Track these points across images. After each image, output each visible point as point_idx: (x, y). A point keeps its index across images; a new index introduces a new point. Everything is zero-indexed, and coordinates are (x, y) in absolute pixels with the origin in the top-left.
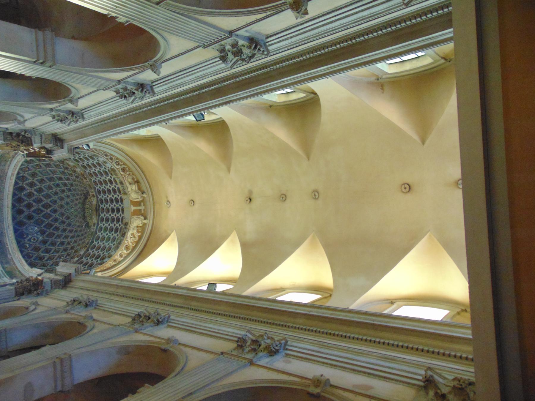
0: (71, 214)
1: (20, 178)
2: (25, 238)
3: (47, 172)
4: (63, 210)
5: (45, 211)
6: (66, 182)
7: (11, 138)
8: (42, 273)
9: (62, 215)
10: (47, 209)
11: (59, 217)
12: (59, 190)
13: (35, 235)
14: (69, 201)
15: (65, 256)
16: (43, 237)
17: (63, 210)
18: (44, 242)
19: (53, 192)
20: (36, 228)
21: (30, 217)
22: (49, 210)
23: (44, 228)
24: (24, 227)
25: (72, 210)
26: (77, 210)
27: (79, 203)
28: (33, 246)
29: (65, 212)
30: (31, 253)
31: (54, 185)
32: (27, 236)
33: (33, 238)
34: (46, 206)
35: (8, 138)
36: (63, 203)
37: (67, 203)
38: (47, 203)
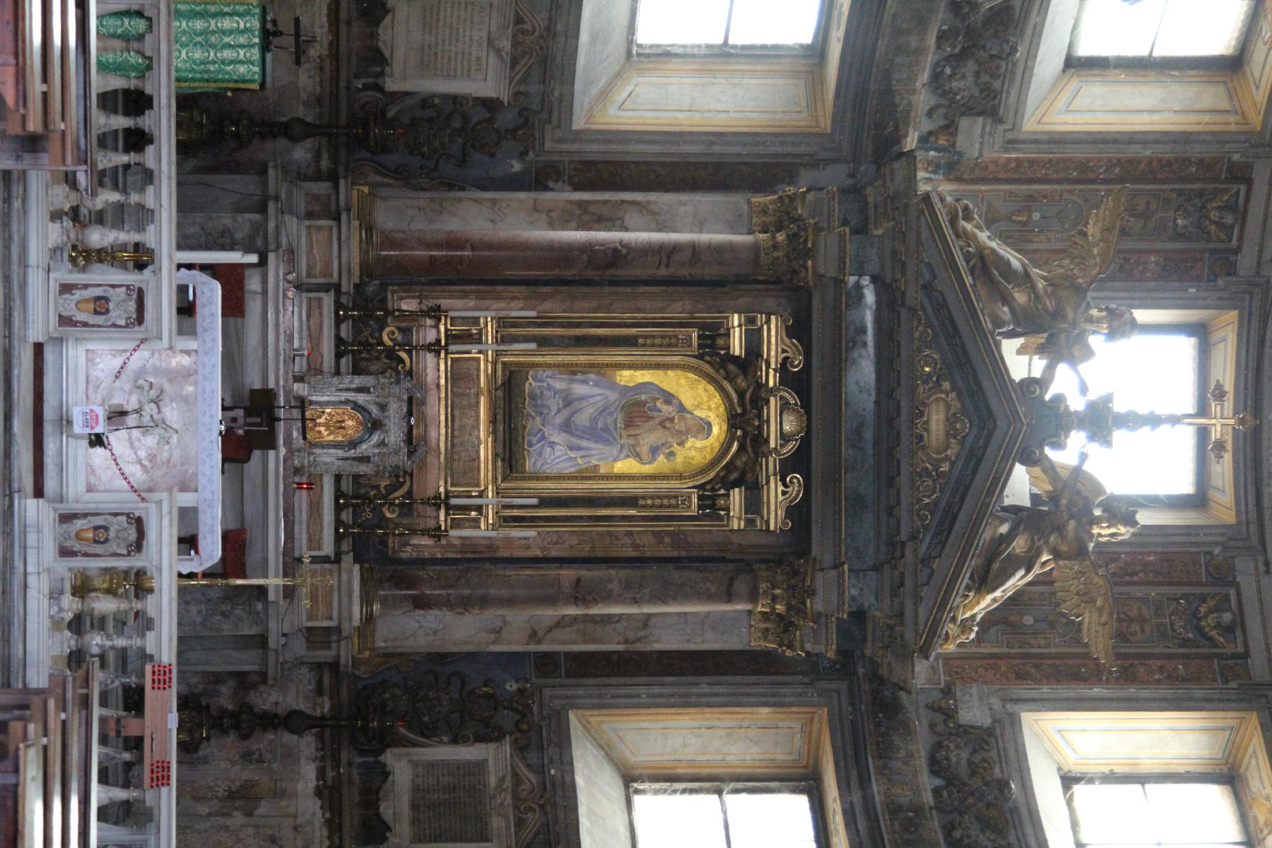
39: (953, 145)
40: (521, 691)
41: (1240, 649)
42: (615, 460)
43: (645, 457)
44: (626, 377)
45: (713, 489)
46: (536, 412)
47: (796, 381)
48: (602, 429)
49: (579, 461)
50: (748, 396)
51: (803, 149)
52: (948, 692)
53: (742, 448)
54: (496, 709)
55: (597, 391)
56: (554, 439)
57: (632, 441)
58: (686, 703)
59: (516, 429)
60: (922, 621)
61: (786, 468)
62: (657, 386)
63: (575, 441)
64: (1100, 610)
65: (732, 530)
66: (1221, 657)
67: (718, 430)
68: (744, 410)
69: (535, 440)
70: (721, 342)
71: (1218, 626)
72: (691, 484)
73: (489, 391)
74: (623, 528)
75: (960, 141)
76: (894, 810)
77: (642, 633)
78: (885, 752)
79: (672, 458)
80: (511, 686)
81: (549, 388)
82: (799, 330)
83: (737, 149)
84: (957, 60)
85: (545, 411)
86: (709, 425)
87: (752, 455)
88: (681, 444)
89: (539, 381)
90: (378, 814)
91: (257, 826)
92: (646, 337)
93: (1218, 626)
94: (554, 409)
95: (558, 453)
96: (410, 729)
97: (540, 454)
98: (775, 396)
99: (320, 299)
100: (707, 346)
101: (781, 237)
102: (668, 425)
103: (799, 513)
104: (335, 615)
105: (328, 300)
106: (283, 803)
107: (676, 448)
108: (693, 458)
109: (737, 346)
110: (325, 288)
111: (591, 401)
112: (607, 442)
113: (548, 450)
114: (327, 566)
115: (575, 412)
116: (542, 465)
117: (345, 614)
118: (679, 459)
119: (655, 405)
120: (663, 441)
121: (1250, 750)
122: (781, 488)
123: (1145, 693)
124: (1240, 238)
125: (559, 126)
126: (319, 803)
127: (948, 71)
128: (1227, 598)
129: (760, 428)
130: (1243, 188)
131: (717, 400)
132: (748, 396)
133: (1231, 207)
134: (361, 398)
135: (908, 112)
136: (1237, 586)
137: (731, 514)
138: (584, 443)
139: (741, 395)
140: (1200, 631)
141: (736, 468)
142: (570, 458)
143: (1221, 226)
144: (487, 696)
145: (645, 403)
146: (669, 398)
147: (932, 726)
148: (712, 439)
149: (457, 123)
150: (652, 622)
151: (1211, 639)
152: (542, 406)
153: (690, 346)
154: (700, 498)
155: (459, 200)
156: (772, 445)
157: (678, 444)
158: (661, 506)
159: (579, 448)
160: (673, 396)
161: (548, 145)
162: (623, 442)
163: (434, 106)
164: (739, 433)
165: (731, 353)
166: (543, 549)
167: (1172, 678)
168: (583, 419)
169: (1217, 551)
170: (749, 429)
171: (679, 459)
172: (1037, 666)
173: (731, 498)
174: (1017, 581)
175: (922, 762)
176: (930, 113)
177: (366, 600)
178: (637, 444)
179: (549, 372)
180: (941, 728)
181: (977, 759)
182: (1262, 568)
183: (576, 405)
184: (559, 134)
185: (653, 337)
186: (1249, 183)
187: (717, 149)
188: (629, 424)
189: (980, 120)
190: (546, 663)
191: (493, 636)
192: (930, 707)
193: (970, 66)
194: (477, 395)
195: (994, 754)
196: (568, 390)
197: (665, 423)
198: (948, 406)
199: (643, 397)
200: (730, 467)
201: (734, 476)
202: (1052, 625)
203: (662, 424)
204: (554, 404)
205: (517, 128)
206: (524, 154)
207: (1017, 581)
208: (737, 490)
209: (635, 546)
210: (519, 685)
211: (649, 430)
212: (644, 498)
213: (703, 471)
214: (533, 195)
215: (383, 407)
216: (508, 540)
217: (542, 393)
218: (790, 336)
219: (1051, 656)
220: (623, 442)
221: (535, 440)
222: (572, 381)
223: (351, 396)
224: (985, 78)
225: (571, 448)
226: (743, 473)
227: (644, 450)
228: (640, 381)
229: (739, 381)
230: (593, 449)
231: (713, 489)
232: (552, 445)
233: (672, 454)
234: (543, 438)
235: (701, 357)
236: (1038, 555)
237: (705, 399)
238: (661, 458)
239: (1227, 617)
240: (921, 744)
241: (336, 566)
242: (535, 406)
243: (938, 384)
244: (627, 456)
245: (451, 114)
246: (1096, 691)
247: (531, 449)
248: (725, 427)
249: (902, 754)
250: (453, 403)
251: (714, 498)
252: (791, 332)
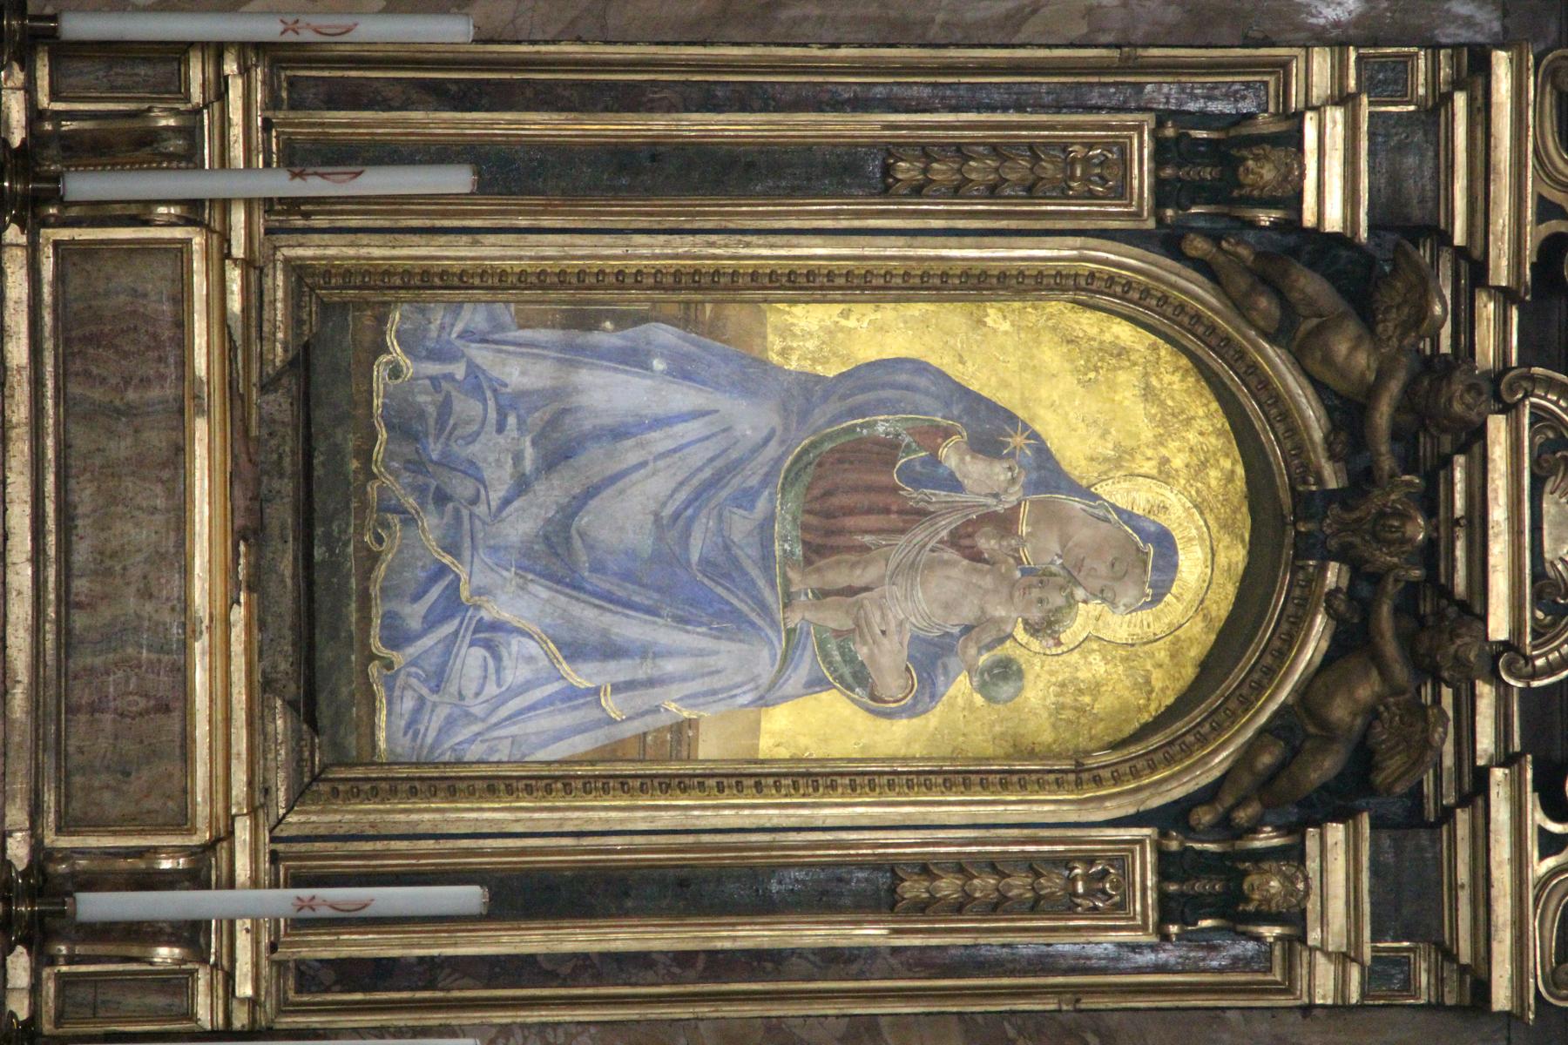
42: (765, 700)
45: (1226, 828)
46: (421, 491)
48: (705, 562)
49: (611, 704)
55: (683, 397)
57: (834, 618)
59: (335, 566)
62: (941, 375)
63: (590, 617)
65: (1308, 1009)
68: (1362, 480)
69: (413, 615)
70: (1263, 172)
72: (1127, 808)
73: (234, 395)
79: (1006, 689)
81: (477, 382)
85: (462, 488)
86: (1164, 542)
87: (1401, 673)
88: (1045, 627)
89: (436, 355)
92: (926, 152)
94: (500, 481)
95: (515, 673)
97: (438, 679)
98: (1509, 409)
100: (1197, 192)
102: (987, 543)
107: (1023, 646)
108: (1095, 688)
111: (660, 440)
112: (729, 622)
113: (472, 659)
115: (591, 492)
116: (450, 723)
118: (1037, 694)
119: (934, 460)
120: (968, 613)
122: (1537, 817)
129: (1432, 554)
137: (1314, 937)
138: (630, 628)
141: (1329, 735)
142: (571, 695)
145: (888, 450)
148: (1174, 607)
152: (447, 463)
153: (1121, 191)
154: (1167, 865)
156: (1499, 627)
157: (1033, 629)
158: (998, 906)
159: (611, 651)
160: (1011, 418)
162: (795, 619)
164: (1333, 575)
165: (1309, 219)
170: (1386, 558)
171: (1037, 694)
173: (1312, 865)
178: (859, 629)
179: (474, 316)
183: (595, 465)
185: (961, 152)
194: (178, 416)
196: (555, 394)
199: (883, 426)
201: (1325, 767)
203: (961, 541)
208: (1336, 833)
211: (911, 568)
212: (925, 868)
217: (445, 408)
220: (795, 619)
221: (413, 615)
222: (573, 356)
225: (575, 651)
226: (1364, 758)
228: (868, 352)
229: (1341, 348)
230: (669, 653)
231: (1226, 828)
232: (491, 634)
233: (1007, 671)
234: (452, 605)
235: (1169, 242)
237: (1147, 433)
238: (961, 687)
242: (417, 465)
244: (816, 684)
247: (399, 658)
248: (1235, 555)
250: (63, 447)
251: (1232, 867)
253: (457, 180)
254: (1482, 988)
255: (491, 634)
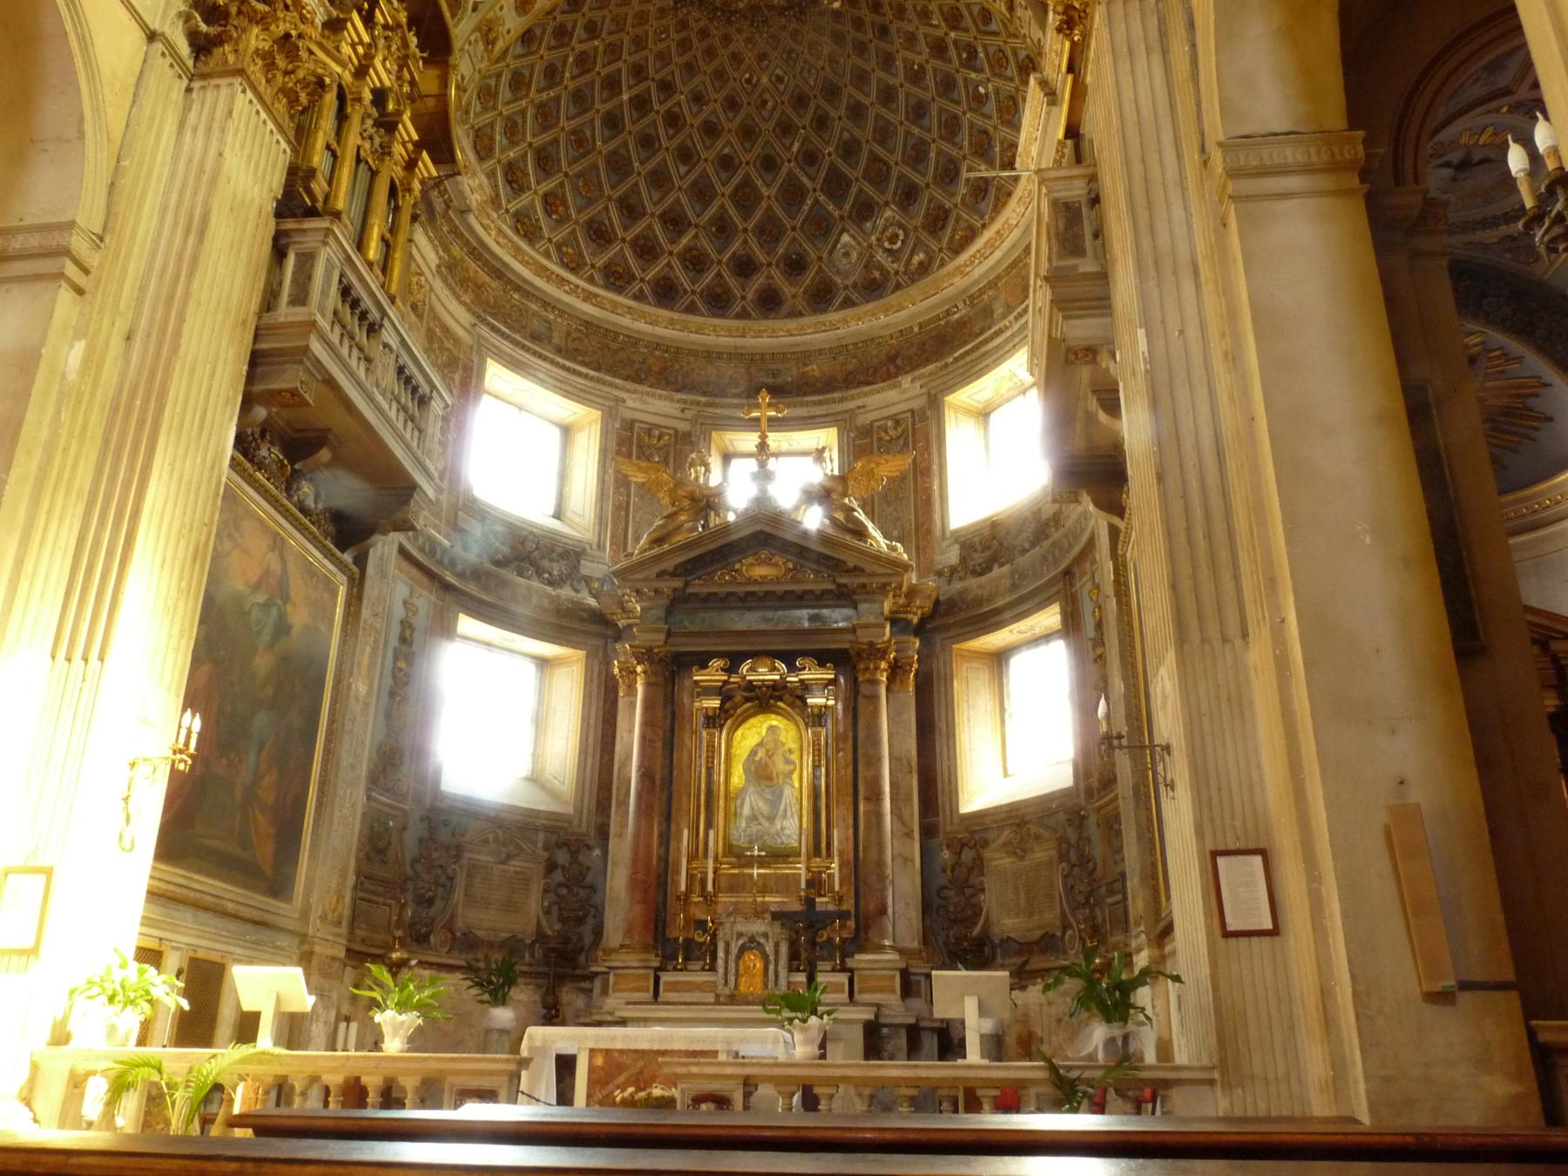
0: (782, 88)
1: (616, 278)
2: (885, 273)
3: (579, 175)
4: (767, 128)
5: (769, 208)
6: (625, 97)
7: (227, 48)
8: (1043, 83)
9: (786, 129)
10: (759, 198)
11: (796, 146)
12: (670, 138)
13: (873, 238)
14: (720, 96)
15: (973, 75)
16: (887, 204)
17: (767, 128)
18: (909, 195)
19: (683, 169)
20: (846, 238)
21: (795, 266)
22: (765, 191)
23: (847, 207)
24: (838, 280)
25: (765, 80)
26: (762, 57)
27: (727, 39)
28: (924, 236)
29: (777, 115)
30: (952, 237)
31: (649, 158)
32: (881, 268)
33: (886, 245)
34: (746, 198)
35: (231, 58)
36: (730, 123)
37: (732, 104)
38: (733, 196)
39: (599, 580)
40: (948, 847)
41: (909, 415)
43: (788, 768)
44: (738, 778)
47: (734, 661)
50: (746, 694)
51: (596, 668)
52: (940, 574)
53: (780, 699)
54: (961, 864)
55: (748, 800)
56: (779, 826)
58: (951, 736)
60: (888, 571)
61: (792, 668)
64: (878, 464)
66: (914, 424)
67: (774, 720)
68: (758, 698)
71: (895, 428)
74: (833, 776)
75: (597, 575)
76: (1014, 587)
77: (905, 761)
78: (979, 602)
80: (946, 854)
81: (745, 831)
82: (702, 661)
83: (593, 709)
84: (539, 572)
88: (783, 744)
90: (1036, 943)
91: (1050, 1034)
93: (895, 428)
96: (975, 924)
97: (789, 837)
99: (665, 983)
101: (639, 669)
103: (822, 658)
104: (892, 973)
105: (666, 977)
106: (1032, 1014)
109: (716, 703)
110: (657, 980)
112: (781, 794)
113: (786, 832)
114: (856, 979)
117: (891, 965)
121: (968, 401)
123: (936, 459)
124: (669, 428)
125: (570, 822)
126: (1031, 988)
127: (546, 575)
128: (879, 427)
129: (768, 687)
130: (637, 425)
131: (753, 721)
132: (746, 694)
133: (649, 432)
134: (734, 950)
135: (572, 602)
136: (872, 422)
138: (782, 807)
139: (747, 700)
140: (899, 438)
143: (660, 438)
144: (953, 870)
146: (753, 752)
147: (961, 579)
148: (781, 725)
149: (564, 891)
150: (896, 754)
151: (903, 431)
154: (814, 726)
155: (611, 888)
156: (778, 677)
158: (819, 750)
159: (785, 810)
161: (583, 829)
163: (550, 906)
166: (848, 828)
167: (927, 448)
168: (763, 807)
169: (852, 435)
172: (923, 524)
174: (861, 515)
175: (983, 579)
176: (577, 591)
177: (880, 949)
180: (962, 574)
181: (980, 548)
182: (862, 410)
184: (576, 822)
186: (633, 421)
187: (592, 722)
188: (769, 778)
189: (582, 562)
190: (928, 832)
191: (909, 863)
192: (949, 582)
193: (545, 563)
194: (743, 875)
195: (977, 540)
197: (770, 755)
198: (751, 565)
199: (753, 768)
200: (792, 705)
201: (798, 703)
202: (898, 519)
203: (770, 757)
204: (754, 829)
205: (570, 850)
206: (589, 847)
207: (861, 515)
209: (846, 766)
210: (945, 848)
213: (797, 725)
214: (611, 837)
215: (740, 935)
216: (841, 853)
218: (707, 667)
219: (916, 518)
223: (732, 957)
224: (554, 556)
225: (785, 816)
227: (788, 768)
232: (783, 828)
233: (790, 751)
235: (722, 726)
236: (845, 505)
239: (890, 423)
240: (973, 582)
241: (856, 973)
243: (736, 571)
245: (557, 894)
246: (936, 487)
248: (773, 716)
249: (979, 592)
252: (704, 665)
253: (711, 833)
254: (830, 680)
255: (783, 828)
